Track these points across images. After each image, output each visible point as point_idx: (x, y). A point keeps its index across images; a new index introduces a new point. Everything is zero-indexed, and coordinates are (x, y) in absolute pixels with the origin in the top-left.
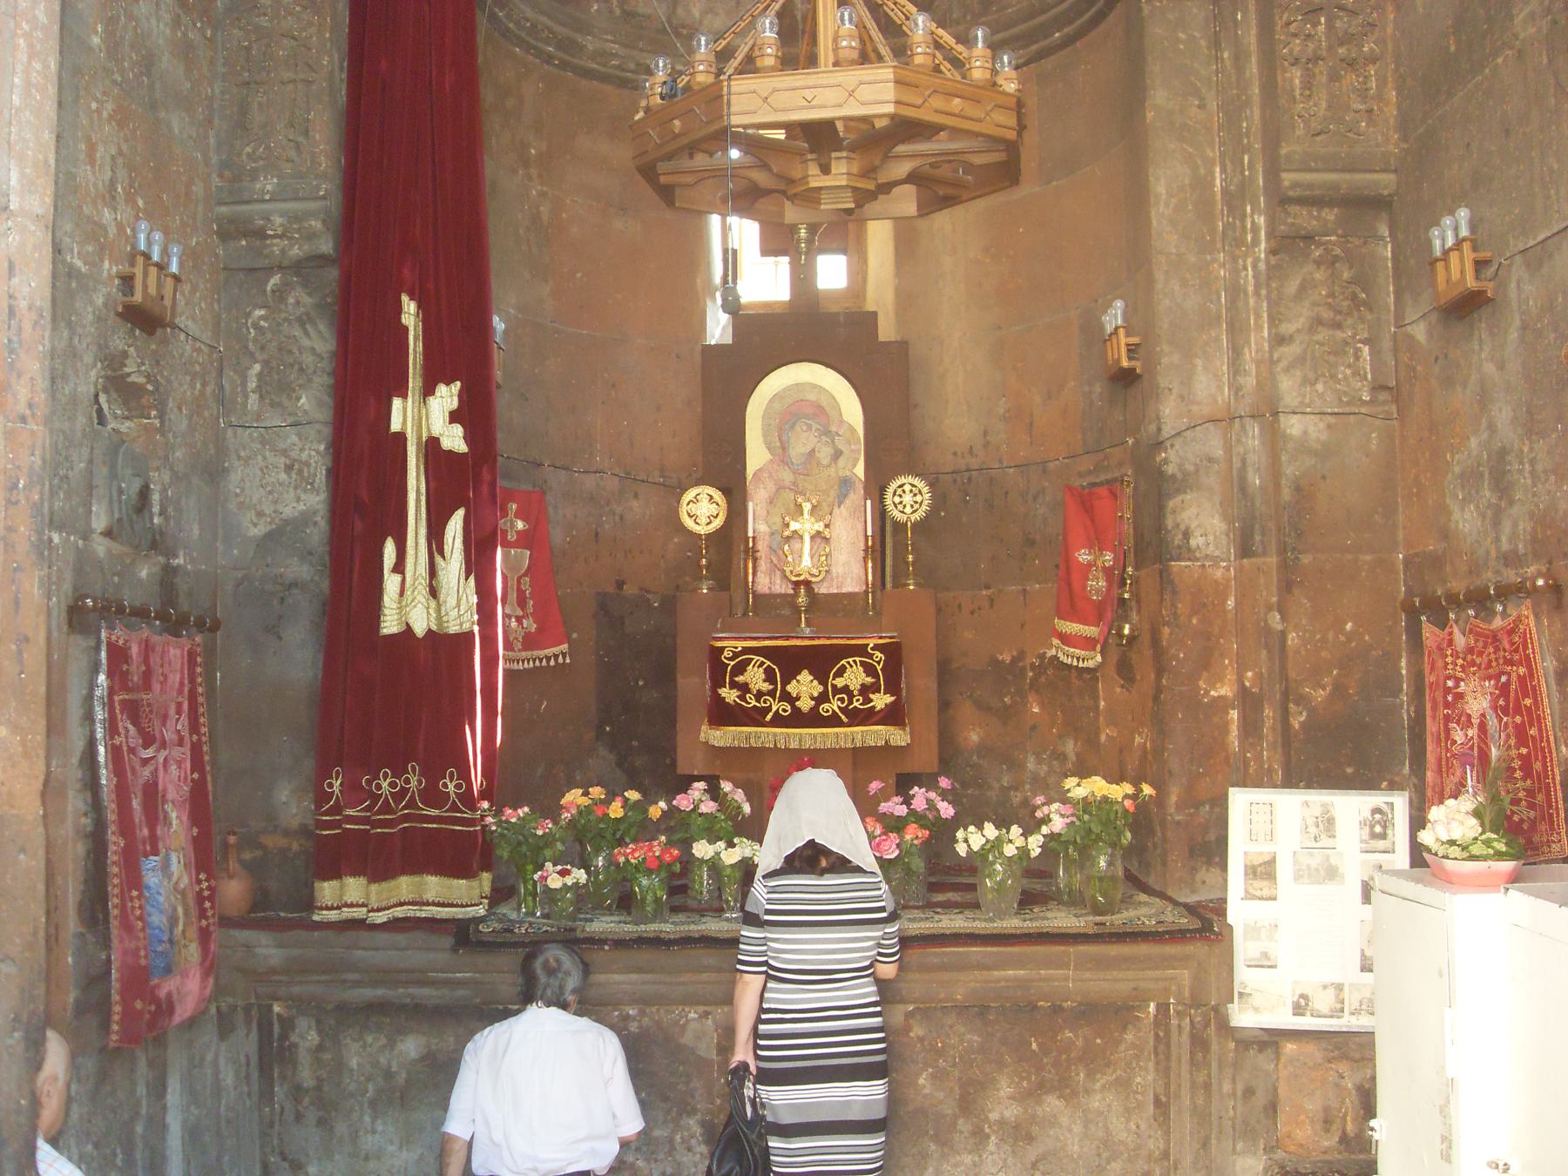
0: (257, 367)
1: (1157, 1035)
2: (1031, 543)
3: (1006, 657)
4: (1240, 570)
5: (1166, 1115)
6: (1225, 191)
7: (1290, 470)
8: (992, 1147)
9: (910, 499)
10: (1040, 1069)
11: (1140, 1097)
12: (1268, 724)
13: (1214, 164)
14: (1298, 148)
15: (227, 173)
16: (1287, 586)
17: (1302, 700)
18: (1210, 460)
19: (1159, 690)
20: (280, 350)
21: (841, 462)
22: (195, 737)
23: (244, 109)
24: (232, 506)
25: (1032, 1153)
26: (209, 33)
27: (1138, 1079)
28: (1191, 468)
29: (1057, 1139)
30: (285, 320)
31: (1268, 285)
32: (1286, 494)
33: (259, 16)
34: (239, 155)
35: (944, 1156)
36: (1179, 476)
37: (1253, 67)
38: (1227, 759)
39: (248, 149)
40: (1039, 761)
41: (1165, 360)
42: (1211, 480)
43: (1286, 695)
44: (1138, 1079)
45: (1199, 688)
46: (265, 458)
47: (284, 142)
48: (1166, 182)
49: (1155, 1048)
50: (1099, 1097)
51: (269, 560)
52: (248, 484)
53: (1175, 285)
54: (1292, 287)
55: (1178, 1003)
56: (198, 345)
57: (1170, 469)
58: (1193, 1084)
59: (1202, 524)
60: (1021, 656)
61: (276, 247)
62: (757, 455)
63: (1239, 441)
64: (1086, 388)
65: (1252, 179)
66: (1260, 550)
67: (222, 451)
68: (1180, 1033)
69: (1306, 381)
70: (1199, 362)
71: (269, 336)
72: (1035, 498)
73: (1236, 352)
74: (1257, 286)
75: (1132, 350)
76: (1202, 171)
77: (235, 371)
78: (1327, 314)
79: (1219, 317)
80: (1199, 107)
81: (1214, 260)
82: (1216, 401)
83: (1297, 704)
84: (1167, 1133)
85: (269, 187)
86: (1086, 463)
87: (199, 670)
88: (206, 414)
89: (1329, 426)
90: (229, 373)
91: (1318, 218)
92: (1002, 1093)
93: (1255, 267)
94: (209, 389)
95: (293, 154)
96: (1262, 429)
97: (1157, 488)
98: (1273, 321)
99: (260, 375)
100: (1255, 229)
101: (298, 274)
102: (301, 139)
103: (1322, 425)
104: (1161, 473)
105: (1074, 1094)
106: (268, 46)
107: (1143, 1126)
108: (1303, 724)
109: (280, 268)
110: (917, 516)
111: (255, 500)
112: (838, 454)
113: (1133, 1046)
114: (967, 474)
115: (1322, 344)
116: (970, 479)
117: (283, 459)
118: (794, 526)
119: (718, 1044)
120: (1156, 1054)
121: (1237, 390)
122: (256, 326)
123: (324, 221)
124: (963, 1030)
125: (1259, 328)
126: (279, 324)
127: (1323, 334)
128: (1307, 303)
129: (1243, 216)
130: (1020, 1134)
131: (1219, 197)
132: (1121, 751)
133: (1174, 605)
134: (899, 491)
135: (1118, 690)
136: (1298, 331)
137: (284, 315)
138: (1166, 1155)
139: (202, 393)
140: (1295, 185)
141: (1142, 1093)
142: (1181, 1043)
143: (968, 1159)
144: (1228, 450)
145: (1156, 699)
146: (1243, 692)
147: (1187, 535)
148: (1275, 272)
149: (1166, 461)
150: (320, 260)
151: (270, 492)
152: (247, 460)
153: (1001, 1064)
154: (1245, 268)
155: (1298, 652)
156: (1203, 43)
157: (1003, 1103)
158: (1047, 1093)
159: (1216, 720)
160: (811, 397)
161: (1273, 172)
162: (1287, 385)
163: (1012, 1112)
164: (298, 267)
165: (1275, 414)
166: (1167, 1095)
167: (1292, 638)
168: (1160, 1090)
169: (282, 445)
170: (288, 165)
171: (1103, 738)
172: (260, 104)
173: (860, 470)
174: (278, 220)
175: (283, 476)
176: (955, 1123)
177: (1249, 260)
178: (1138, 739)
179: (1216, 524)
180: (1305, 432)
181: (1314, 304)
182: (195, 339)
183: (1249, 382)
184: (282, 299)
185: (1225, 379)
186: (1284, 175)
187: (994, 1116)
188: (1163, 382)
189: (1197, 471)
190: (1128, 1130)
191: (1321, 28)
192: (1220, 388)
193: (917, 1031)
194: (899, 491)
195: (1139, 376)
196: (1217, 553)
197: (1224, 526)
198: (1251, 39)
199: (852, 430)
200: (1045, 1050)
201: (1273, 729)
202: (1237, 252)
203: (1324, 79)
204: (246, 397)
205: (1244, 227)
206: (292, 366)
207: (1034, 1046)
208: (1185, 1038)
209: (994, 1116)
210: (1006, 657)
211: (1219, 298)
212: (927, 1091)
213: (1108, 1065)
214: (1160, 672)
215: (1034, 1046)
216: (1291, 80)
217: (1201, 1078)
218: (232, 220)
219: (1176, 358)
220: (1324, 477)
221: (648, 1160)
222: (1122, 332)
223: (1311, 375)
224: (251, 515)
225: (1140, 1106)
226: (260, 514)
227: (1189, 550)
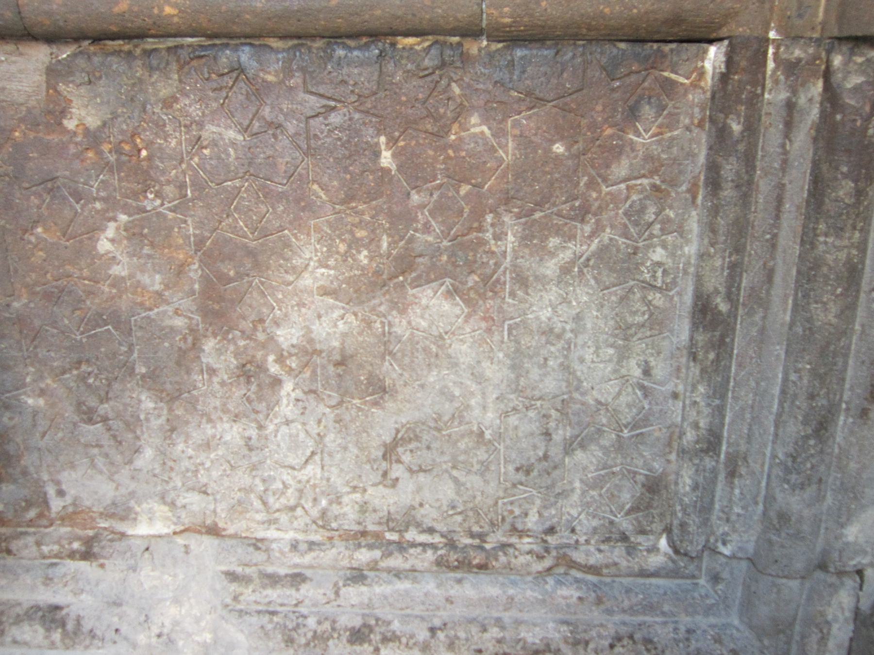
1: (721, 135)
5: (722, 346)
8: (286, 409)
10: (401, 219)
11: (657, 299)
25: (385, 422)
27: (658, 254)
29: (445, 394)
44: (658, 254)
49: (713, 168)
50: (553, 293)
55: (792, 37)
58: (809, 272)
68: (789, 125)
84: (720, 392)
92: (307, 281)
105: (490, 285)
107: (660, 370)
113: (652, 164)
120: (714, 183)
124: (195, 111)
130: (352, 378)
138: (711, 443)
141: (664, 290)
143: (232, 433)
153: (303, 205)
157: (309, 301)
158: (417, 283)
163: (332, 325)
166: (730, 297)
168: (715, 282)
176: (196, 346)
187: (288, 336)
190: (625, 379)
193: (83, 114)
200: (413, 169)
207: (386, 159)
208: (802, 142)
209: (288, 336)
212: (117, 270)
213: (582, 214)
215: (386, 159)
217: (833, 250)
225: (657, 322)
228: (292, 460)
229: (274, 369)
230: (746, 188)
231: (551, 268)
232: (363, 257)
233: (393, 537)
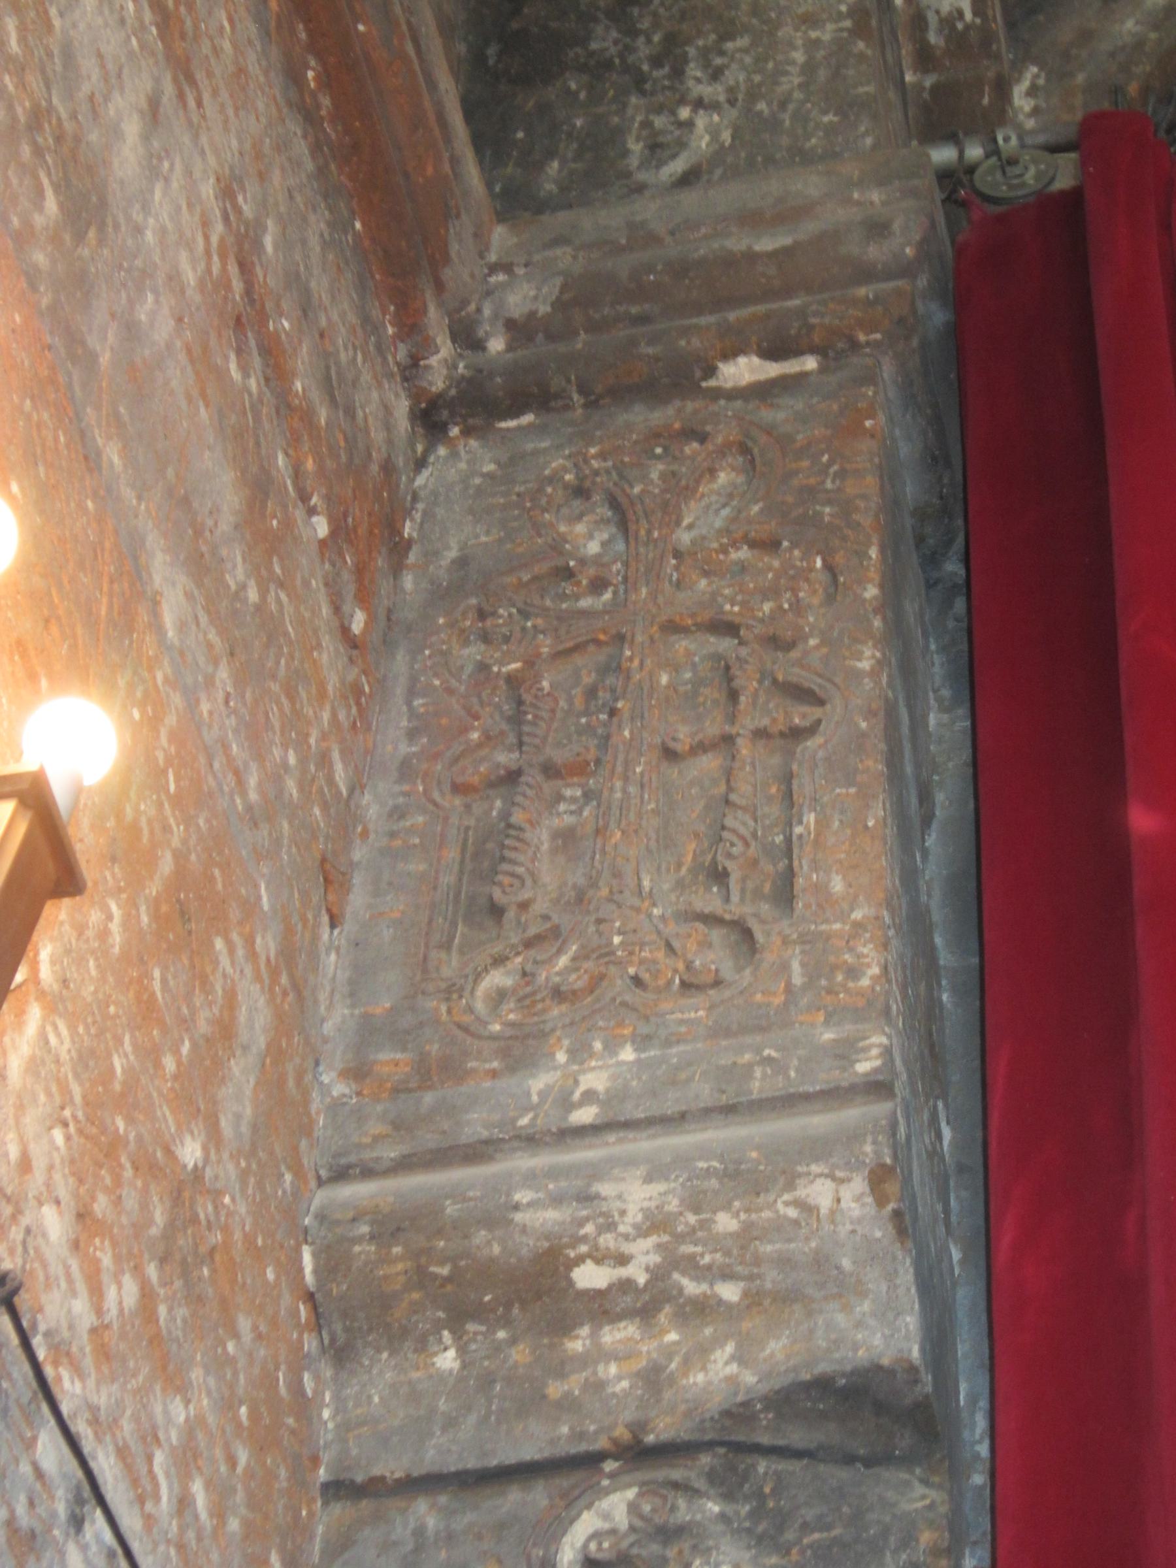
15: (390, 1060)
23: (490, 853)
39: (497, 979)
61: (612, 1364)
95: (714, 955)
101: (727, 1483)
106: (613, 667)
109: (639, 1453)
123: (878, 1178)
150: (862, 1414)
164: (730, 1445)
172: (566, 839)
174: (634, 1196)
218: (389, 1226)
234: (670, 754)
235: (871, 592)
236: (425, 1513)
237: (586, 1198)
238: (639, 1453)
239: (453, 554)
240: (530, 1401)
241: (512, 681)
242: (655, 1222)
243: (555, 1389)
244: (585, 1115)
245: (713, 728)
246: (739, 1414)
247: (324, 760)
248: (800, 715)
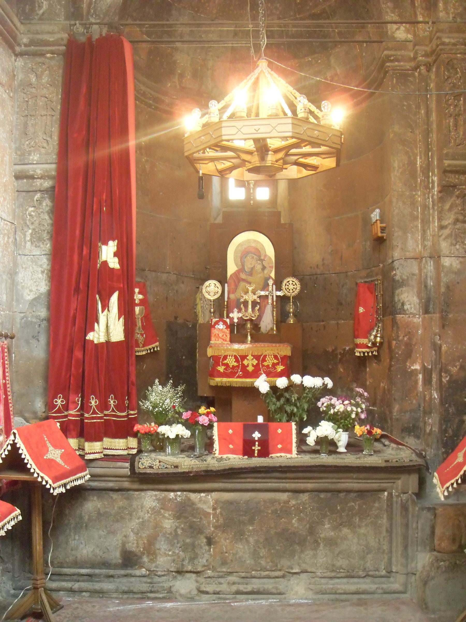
0: (30, 231)
2: (341, 304)
3: (330, 349)
4: (424, 320)
6: (421, 167)
7: (444, 280)
8: (321, 548)
9: (292, 286)
12: (434, 380)
13: (417, 155)
14: (451, 151)
15: (19, 153)
16: (443, 326)
17: (447, 371)
18: (413, 275)
19: (391, 366)
20: (40, 224)
21: (266, 272)
22: (4, 381)
23: (26, 125)
24: (19, 287)
25: (337, 550)
26: (11, 94)
28: (406, 278)
30: (42, 212)
31: (438, 205)
32: (443, 290)
33: (32, 88)
34: (23, 145)
35: (302, 552)
36: (401, 281)
37: (434, 117)
38: (417, 394)
39: (27, 143)
40: (342, 391)
41: (396, 234)
42: (414, 283)
43: (441, 371)
44: (380, 522)
45: (407, 365)
46: (33, 268)
47: (42, 140)
48: (397, 163)
50: (364, 528)
51: (34, 310)
52: (26, 279)
53: (400, 204)
54: (447, 206)
56: (6, 222)
57: (397, 278)
59: (409, 299)
60: (336, 349)
62: (232, 268)
63: (425, 267)
64: (364, 243)
65: (433, 161)
66: (432, 311)
67: (15, 264)
69: (452, 244)
70: (409, 235)
71: (35, 218)
72: (343, 286)
73: (424, 232)
74: (433, 205)
75: (383, 229)
76: (412, 158)
77: (21, 233)
78: (461, 217)
79: (418, 217)
80: (411, 132)
81: (417, 194)
82: (415, 250)
83: (446, 372)
85: (36, 158)
86: (364, 273)
87: (6, 354)
88: (9, 250)
89: (461, 262)
90: (18, 233)
91: (458, 179)
93: (432, 198)
94: (10, 240)
95: (45, 145)
96: (434, 263)
97: (391, 285)
98: (440, 219)
99: (31, 234)
100: (433, 182)
102: (48, 139)
103: (458, 262)
104: (393, 280)
105: (355, 527)
106: (36, 100)
108: (448, 381)
109: (40, 191)
110: (293, 294)
111: (29, 285)
112: (264, 268)
114: (315, 276)
115: (459, 229)
116: (317, 278)
117: (40, 269)
118: (246, 297)
119: (213, 506)
121: (424, 247)
122: (30, 215)
125: (434, 222)
126: (39, 214)
127: (459, 225)
128: (453, 213)
129: (428, 177)
130: (331, 543)
131: (419, 169)
132: (375, 389)
133: (397, 332)
134: (288, 284)
135: (374, 364)
136: (449, 224)
137: (41, 210)
139: (8, 242)
140: (449, 165)
142: (397, 508)
143: (311, 553)
144: (420, 270)
145: (389, 369)
146: (424, 369)
147: (403, 304)
148: (442, 200)
149: (395, 275)
151: (35, 282)
152: (26, 268)
153: (325, 516)
154: (429, 198)
155: (446, 352)
156: (414, 106)
157: (326, 530)
159: (413, 378)
160: (253, 245)
161: (440, 160)
162: (444, 246)
165: (439, 257)
167: (444, 348)
169: (40, 263)
170: (43, 149)
171: (368, 383)
172: (32, 124)
173: (273, 275)
175: (40, 275)
177: (431, 195)
178: (382, 385)
179: (415, 300)
180: (451, 265)
181: (456, 213)
182: (5, 220)
183: (429, 244)
184: (40, 204)
185: (420, 242)
186: (445, 161)
188: (395, 243)
189: (408, 279)
191: (461, 102)
192: (418, 246)
194: (288, 284)
195: (385, 240)
196: (415, 312)
197: (418, 301)
198: (433, 105)
199: (270, 258)
200: (343, 510)
201: (436, 383)
202: (425, 191)
203: (462, 123)
204: (25, 243)
205: (429, 181)
206: (44, 230)
209: (322, 536)
210: (330, 349)
211: (418, 209)
212: (295, 525)
213: (368, 516)
214: (391, 360)
216: (449, 123)
218: (21, 172)
219: (400, 233)
220: (458, 283)
221: (183, 551)
222: (378, 222)
223: (454, 242)
224: (27, 291)
226: (31, 291)
227: (404, 310)
228: (322, 557)
229: (319, 541)
230: (392, 513)
231: (363, 524)
232: (335, 523)
233: (338, 571)
234: (41, 116)
235: (60, 97)
236: (24, 194)
237: (35, 171)
238: (40, 191)
239: (20, 79)
240: (31, 186)
241: (27, 101)
242: (41, 174)
243: (33, 184)
244: (35, 162)
245: (45, 113)
246: (47, 188)
247: (10, 119)
248: (53, 113)
